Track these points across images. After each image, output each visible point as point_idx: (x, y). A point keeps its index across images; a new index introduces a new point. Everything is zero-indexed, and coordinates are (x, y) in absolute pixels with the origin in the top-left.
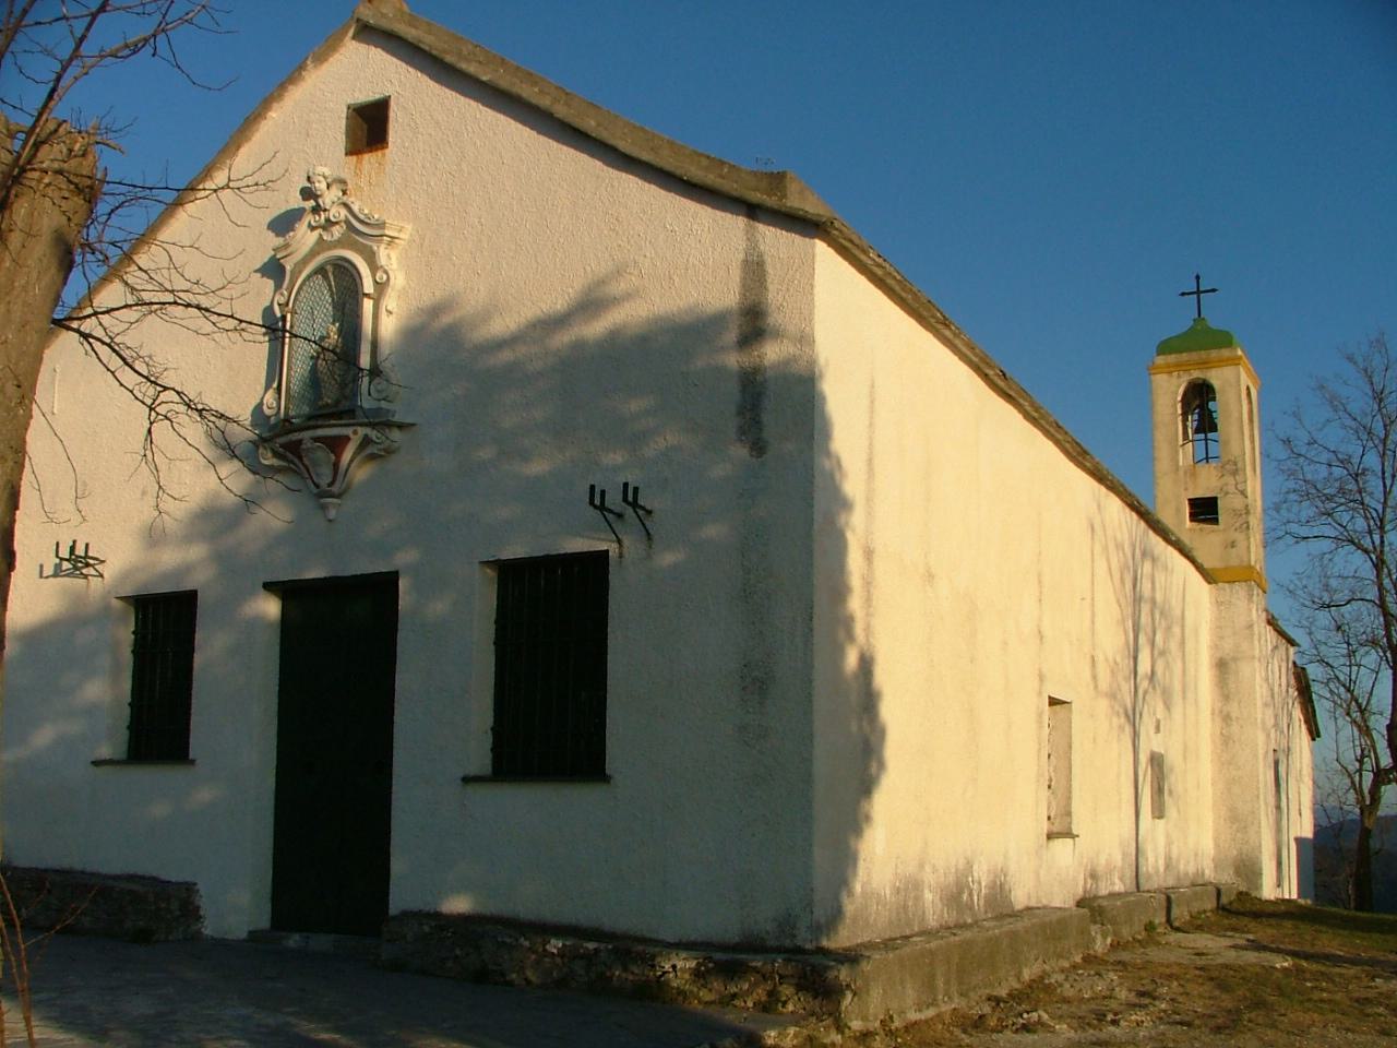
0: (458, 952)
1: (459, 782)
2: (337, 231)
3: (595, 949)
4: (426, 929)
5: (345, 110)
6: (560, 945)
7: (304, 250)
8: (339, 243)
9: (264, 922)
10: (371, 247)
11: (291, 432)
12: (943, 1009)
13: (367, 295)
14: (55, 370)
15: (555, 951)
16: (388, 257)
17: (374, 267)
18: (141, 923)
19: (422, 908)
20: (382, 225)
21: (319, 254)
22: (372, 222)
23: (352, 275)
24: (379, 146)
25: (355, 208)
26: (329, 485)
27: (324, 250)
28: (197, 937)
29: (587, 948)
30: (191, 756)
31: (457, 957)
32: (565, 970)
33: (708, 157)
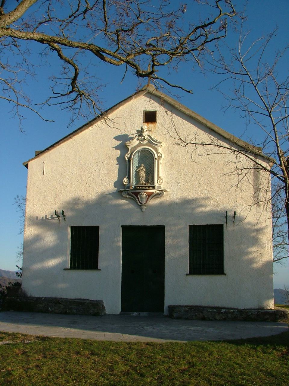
0: (196, 314)
1: (186, 275)
2: (145, 142)
3: (233, 311)
4: (187, 309)
5: (143, 112)
6: (225, 311)
7: (135, 144)
8: (146, 145)
9: (275, 287)
10: (156, 147)
11: (136, 190)
12: (194, 360)
13: (156, 159)
14: (44, 163)
15: (223, 312)
16: (160, 150)
17: (158, 153)
18: (96, 311)
19: (175, 304)
20: (161, 143)
21: (140, 146)
22: (157, 141)
23: (151, 153)
24: (154, 122)
25: (153, 137)
26: (145, 203)
27: (141, 146)
28: (105, 314)
29: (231, 311)
30: (99, 268)
31: (196, 315)
32: (225, 316)
33: (243, 141)
